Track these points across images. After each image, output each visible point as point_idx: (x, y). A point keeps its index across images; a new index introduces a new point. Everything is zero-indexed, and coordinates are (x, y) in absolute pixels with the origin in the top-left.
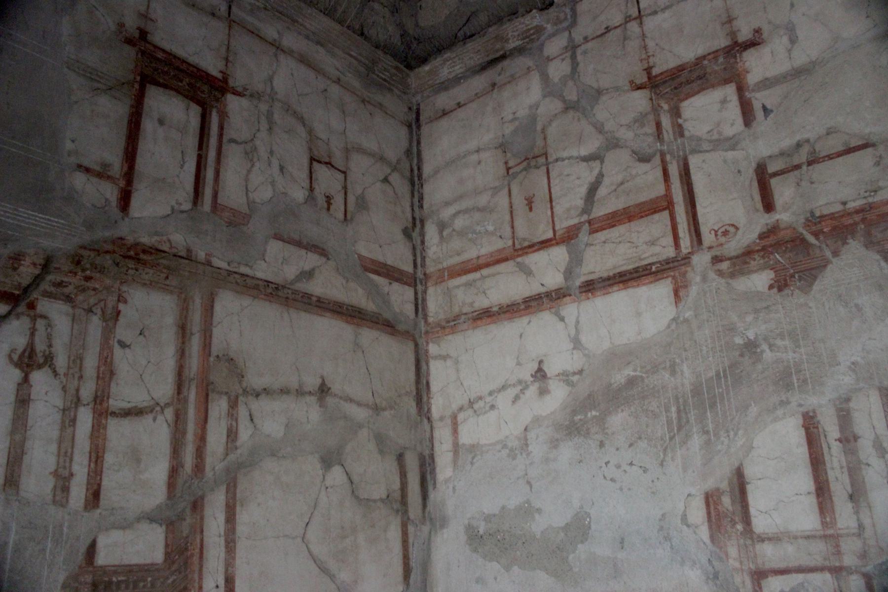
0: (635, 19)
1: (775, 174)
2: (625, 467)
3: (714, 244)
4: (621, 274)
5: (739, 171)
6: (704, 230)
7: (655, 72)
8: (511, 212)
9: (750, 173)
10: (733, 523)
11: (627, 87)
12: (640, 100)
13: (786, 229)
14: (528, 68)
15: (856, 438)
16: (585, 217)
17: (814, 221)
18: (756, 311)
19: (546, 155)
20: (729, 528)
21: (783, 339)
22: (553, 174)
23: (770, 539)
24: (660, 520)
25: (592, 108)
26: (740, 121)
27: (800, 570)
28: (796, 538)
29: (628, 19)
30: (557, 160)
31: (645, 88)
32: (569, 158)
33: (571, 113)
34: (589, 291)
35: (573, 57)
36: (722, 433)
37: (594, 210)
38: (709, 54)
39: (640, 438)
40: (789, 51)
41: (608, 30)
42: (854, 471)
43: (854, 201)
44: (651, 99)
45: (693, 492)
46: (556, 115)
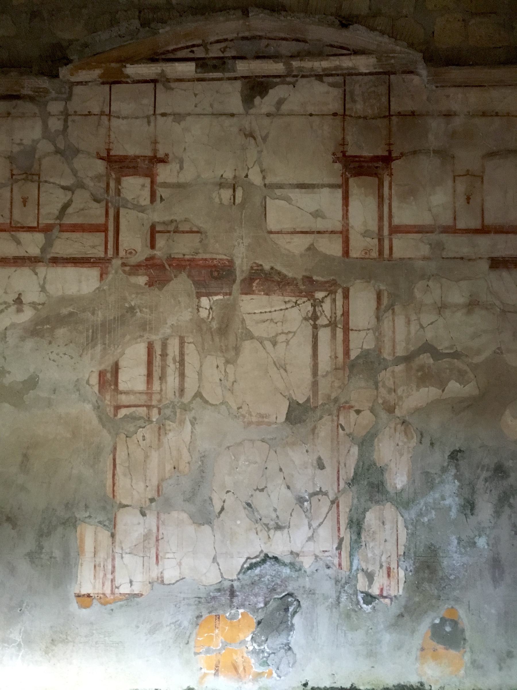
0: (106, 115)
1: (159, 232)
2: (61, 355)
3: (124, 257)
4: (74, 259)
5: (143, 225)
7: (112, 153)
8: (11, 203)
9: (147, 227)
10: (110, 385)
11: (95, 154)
12: (100, 166)
13: (159, 259)
14: (35, 113)
16: (58, 222)
17: (170, 259)
18: (137, 293)
19: (39, 175)
20: (108, 387)
21: (146, 308)
22: (42, 189)
23: (125, 393)
24: (76, 381)
25: (72, 159)
28: (136, 393)
29: (102, 113)
30: (46, 182)
31: (104, 160)
32: (53, 183)
33: (59, 156)
34: (54, 262)
35: (66, 121)
36: (112, 345)
37: (64, 219)
38: (141, 156)
39: (71, 342)
40: (178, 173)
41: (90, 114)
42: (163, 368)
43: (188, 255)
44: (107, 168)
45: (94, 370)
46: (49, 153)
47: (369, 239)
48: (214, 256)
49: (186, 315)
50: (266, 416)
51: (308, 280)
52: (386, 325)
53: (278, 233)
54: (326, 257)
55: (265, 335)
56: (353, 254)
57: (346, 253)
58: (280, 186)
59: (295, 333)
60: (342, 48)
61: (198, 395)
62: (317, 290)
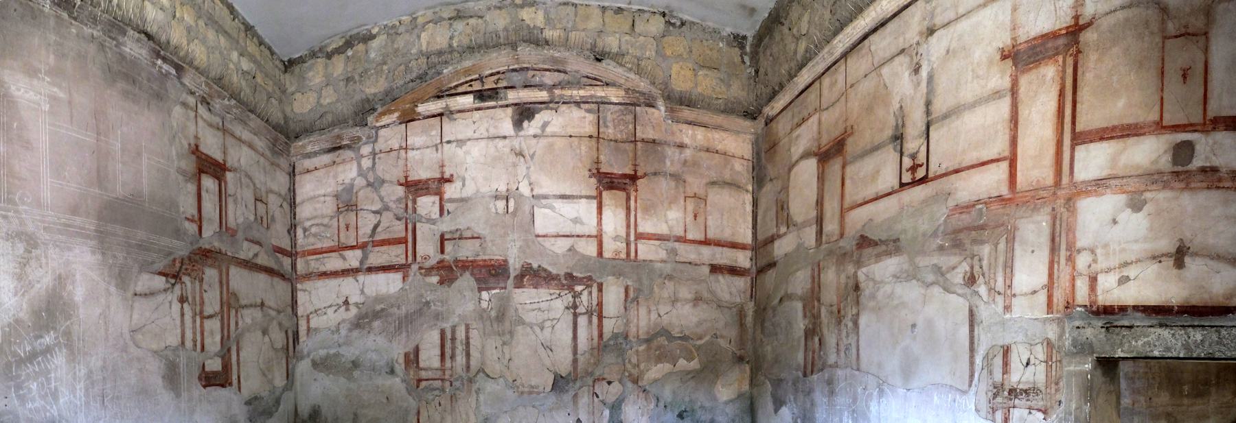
6: (418, 256)
9: (438, 237)
15: (456, 339)
17: (456, 261)
18: (431, 291)
26: (438, 213)
27: (432, 379)
42: (453, 349)
47: (619, 243)
48: (492, 257)
49: (471, 306)
50: (537, 387)
51: (570, 276)
52: (633, 313)
53: (544, 236)
54: (584, 256)
55: (535, 322)
56: (607, 254)
57: (600, 254)
58: (545, 197)
59: (559, 319)
60: (595, 79)
61: (481, 370)
62: (577, 284)
